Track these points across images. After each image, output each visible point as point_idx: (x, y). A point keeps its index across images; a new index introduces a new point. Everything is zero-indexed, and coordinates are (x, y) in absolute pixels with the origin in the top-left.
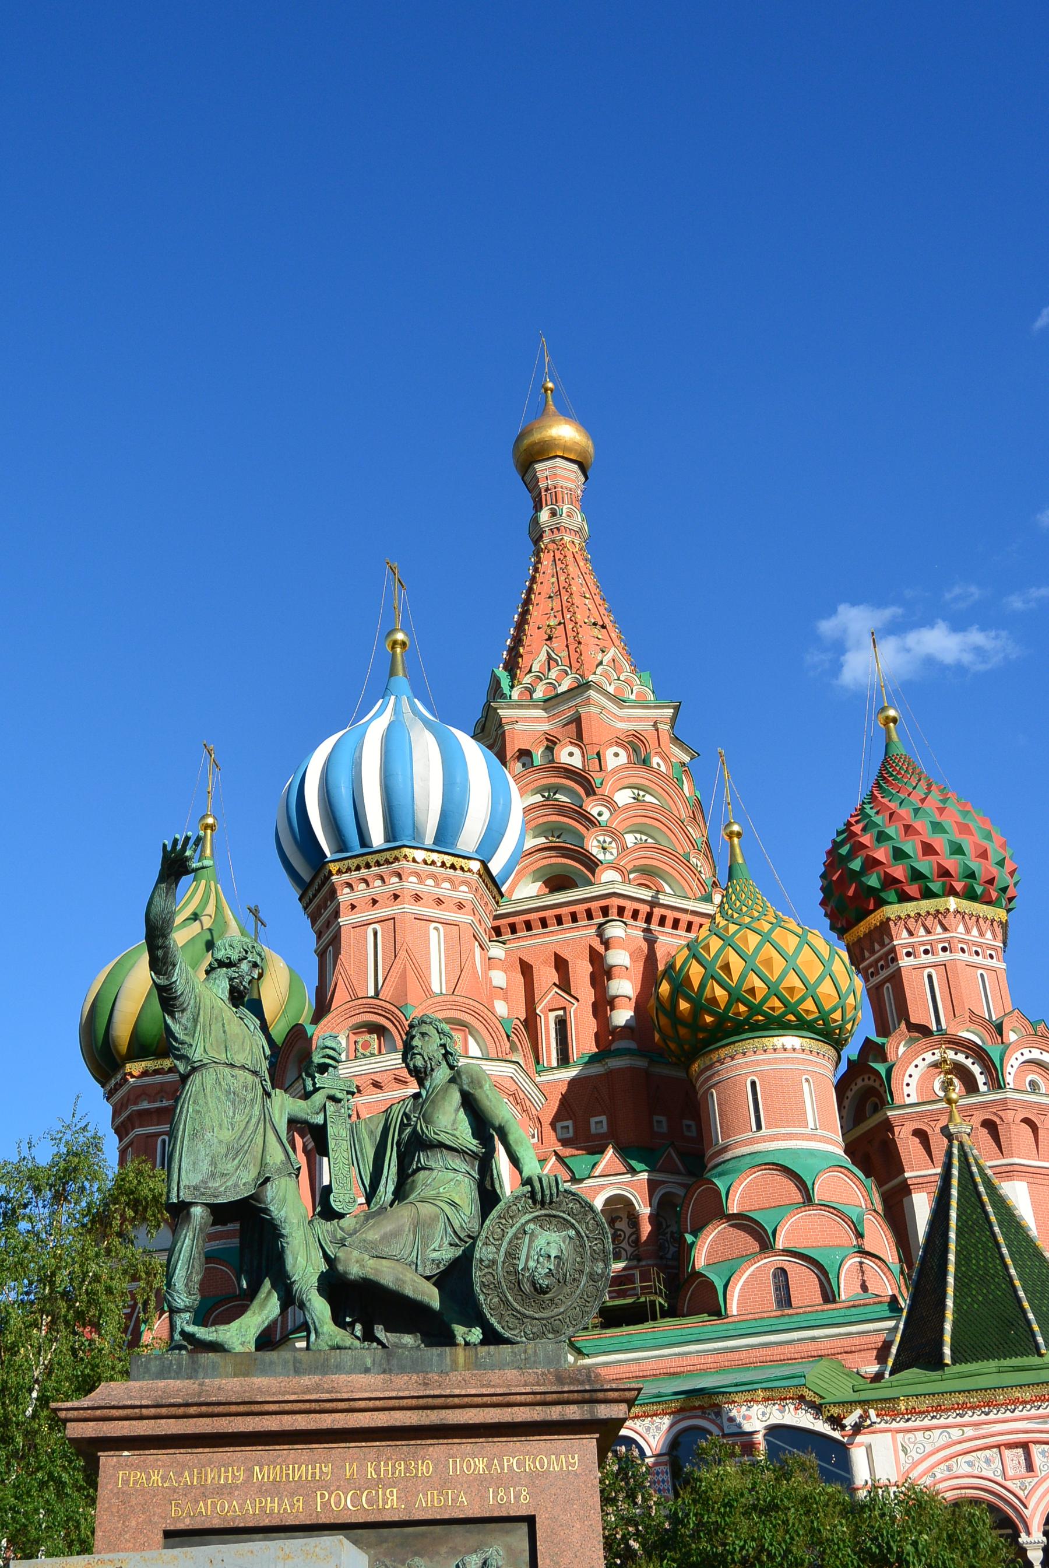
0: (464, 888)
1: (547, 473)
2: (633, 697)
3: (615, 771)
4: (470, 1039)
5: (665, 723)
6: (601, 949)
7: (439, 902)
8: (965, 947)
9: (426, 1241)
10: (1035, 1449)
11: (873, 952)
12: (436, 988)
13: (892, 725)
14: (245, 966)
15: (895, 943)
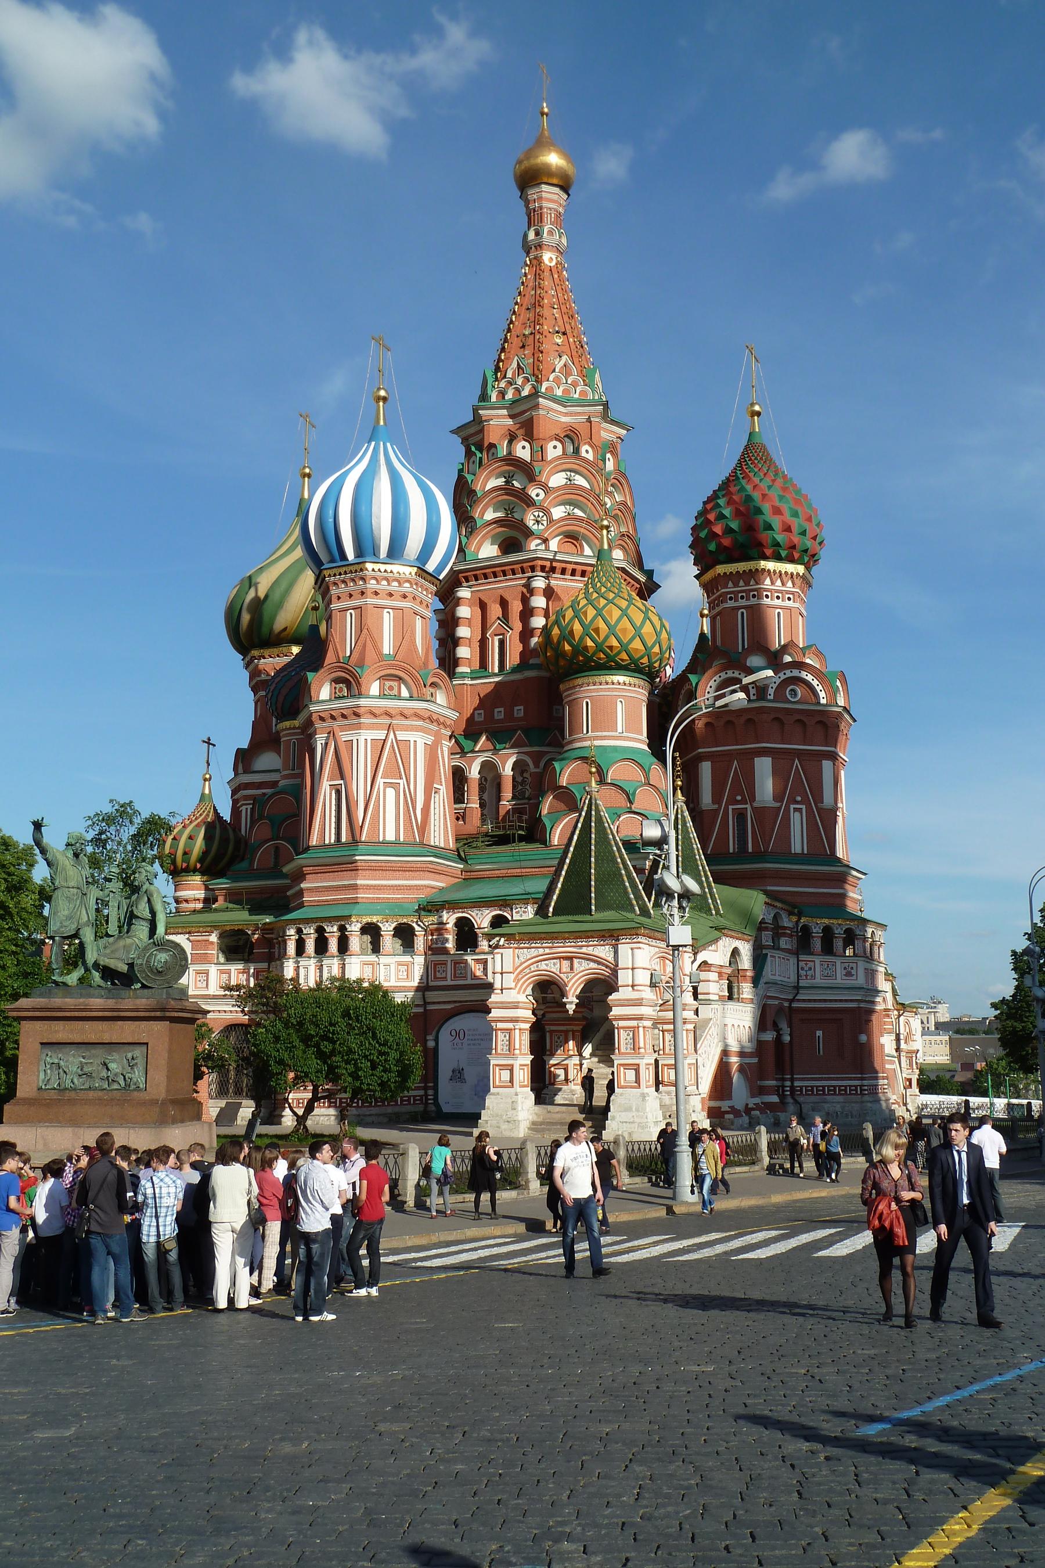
0: (407, 585)
1: (535, 197)
2: (576, 396)
3: (551, 462)
4: (403, 686)
5: (597, 417)
6: (528, 595)
7: (391, 595)
8: (769, 594)
9: (128, 952)
10: (576, 961)
11: (713, 594)
12: (386, 651)
13: (756, 417)
14: (78, 845)
15: (723, 590)
